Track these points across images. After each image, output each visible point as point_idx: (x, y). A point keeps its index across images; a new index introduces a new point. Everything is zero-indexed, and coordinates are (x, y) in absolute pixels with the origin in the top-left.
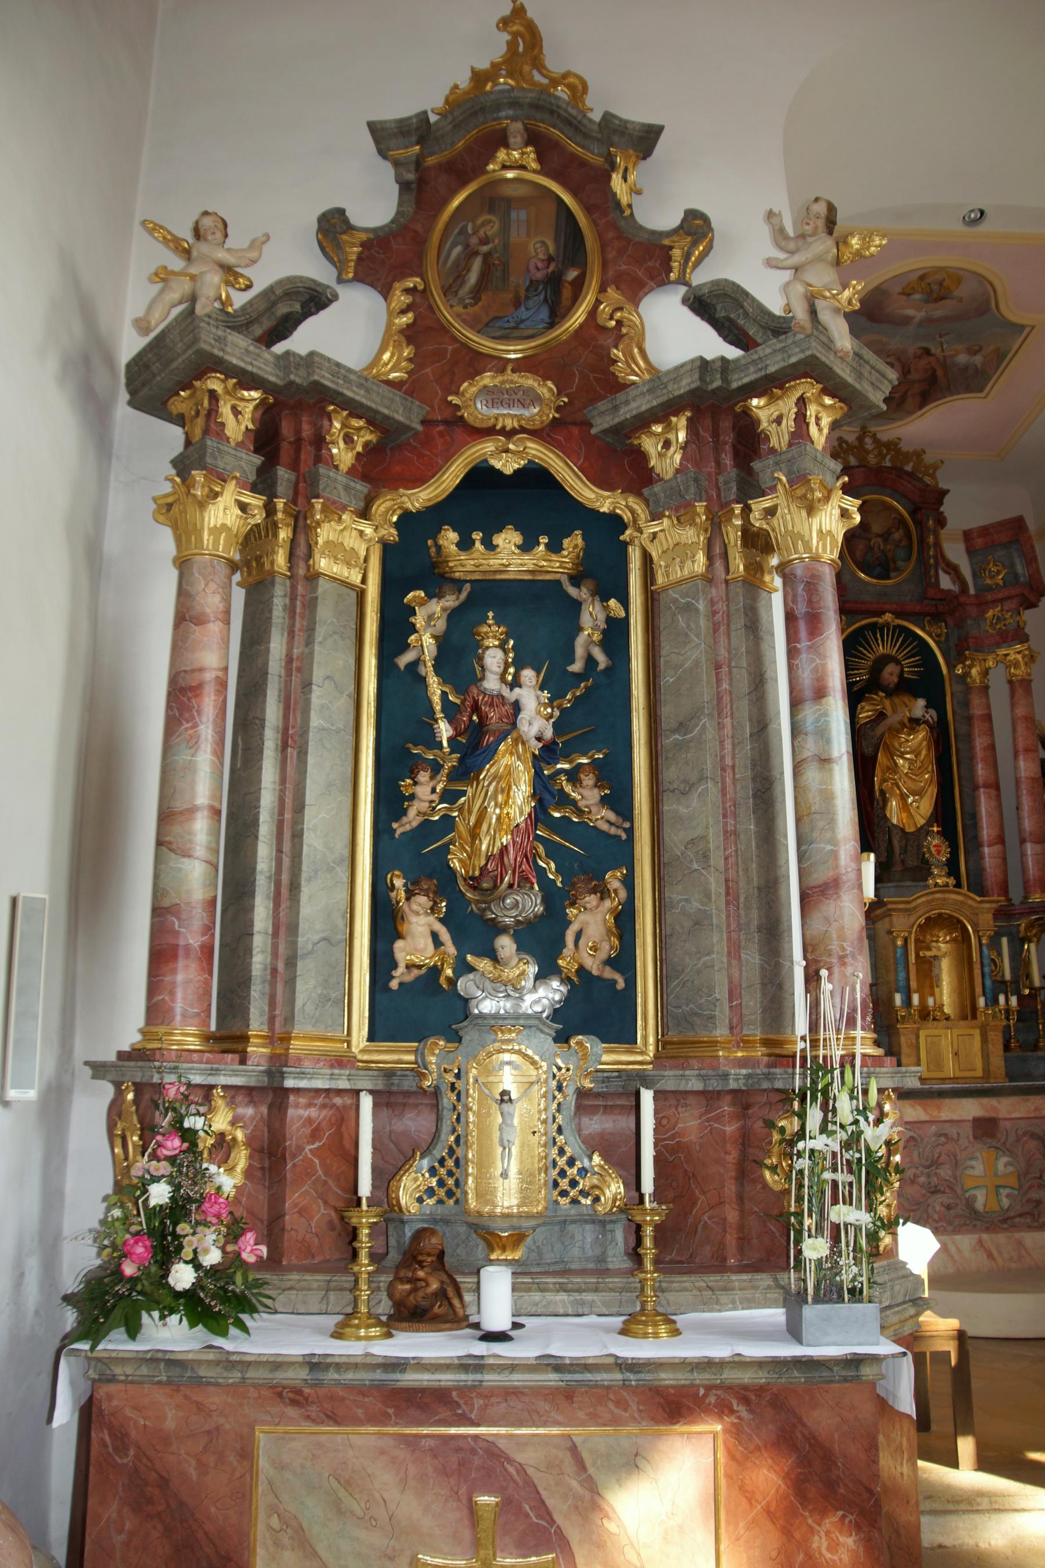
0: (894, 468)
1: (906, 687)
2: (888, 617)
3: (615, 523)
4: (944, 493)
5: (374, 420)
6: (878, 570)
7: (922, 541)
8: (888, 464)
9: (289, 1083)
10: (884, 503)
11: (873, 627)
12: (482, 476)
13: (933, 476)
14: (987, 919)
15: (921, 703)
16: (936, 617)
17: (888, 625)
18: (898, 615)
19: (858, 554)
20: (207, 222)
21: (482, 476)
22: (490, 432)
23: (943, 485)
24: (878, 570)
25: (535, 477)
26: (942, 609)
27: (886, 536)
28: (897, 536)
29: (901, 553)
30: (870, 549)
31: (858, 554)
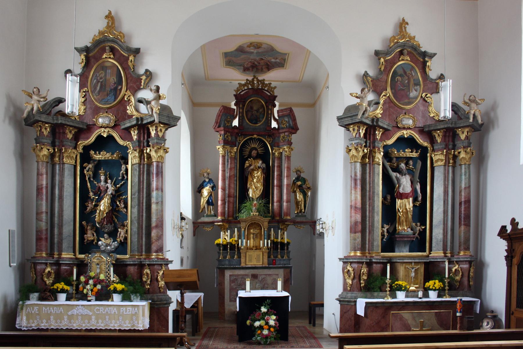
0: (262, 89)
1: (258, 157)
2: (255, 136)
3: (126, 148)
4: (276, 96)
5: (75, 127)
6: (254, 121)
7: (267, 112)
8: (260, 87)
9: (61, 262)
10: (258, 100)
11: (251, 139)
12: (100, 137)
13: (273, 92)
14: (266, 224)
15: (261, 162)
16: (269, 136)
17: (254, 138)
18: (258, 135)
19: (249, 117)
20: (35, 90)
21: (100, 137)
22: (101, 127)
23: (275, 94)
24: (254, 121)
25: (110, 137)
26: (272, 133)
27: (257, 111)
28: (261, 110)
29: (261, 116)
30: (253, 115)
31: (249, 117)
